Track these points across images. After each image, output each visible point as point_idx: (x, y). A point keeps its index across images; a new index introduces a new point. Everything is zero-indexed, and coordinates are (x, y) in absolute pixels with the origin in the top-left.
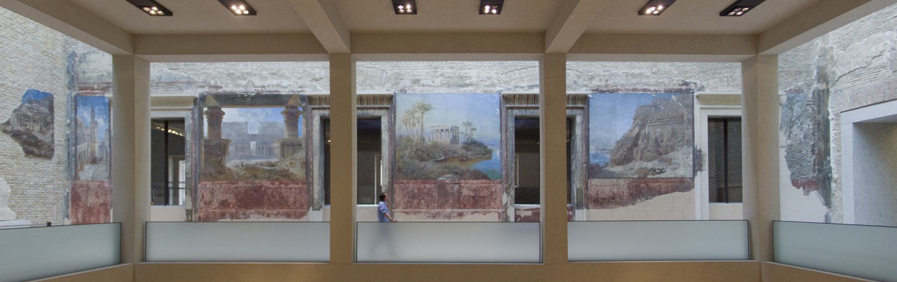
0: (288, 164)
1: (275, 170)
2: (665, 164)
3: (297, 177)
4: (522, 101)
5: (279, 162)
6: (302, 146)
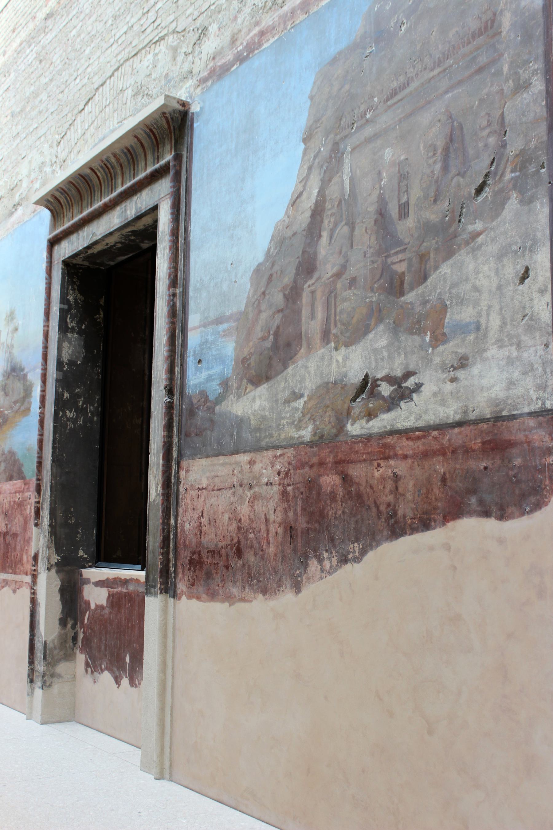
2: (417, 338)
4: (74, 207)
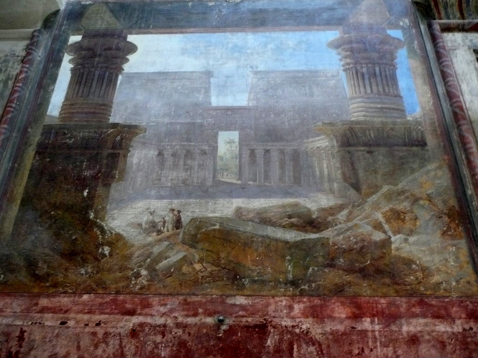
0: (379, 216)
1: (324, 243)
3: (436, 278)
5: (341, 208)
6: (428, 148)
